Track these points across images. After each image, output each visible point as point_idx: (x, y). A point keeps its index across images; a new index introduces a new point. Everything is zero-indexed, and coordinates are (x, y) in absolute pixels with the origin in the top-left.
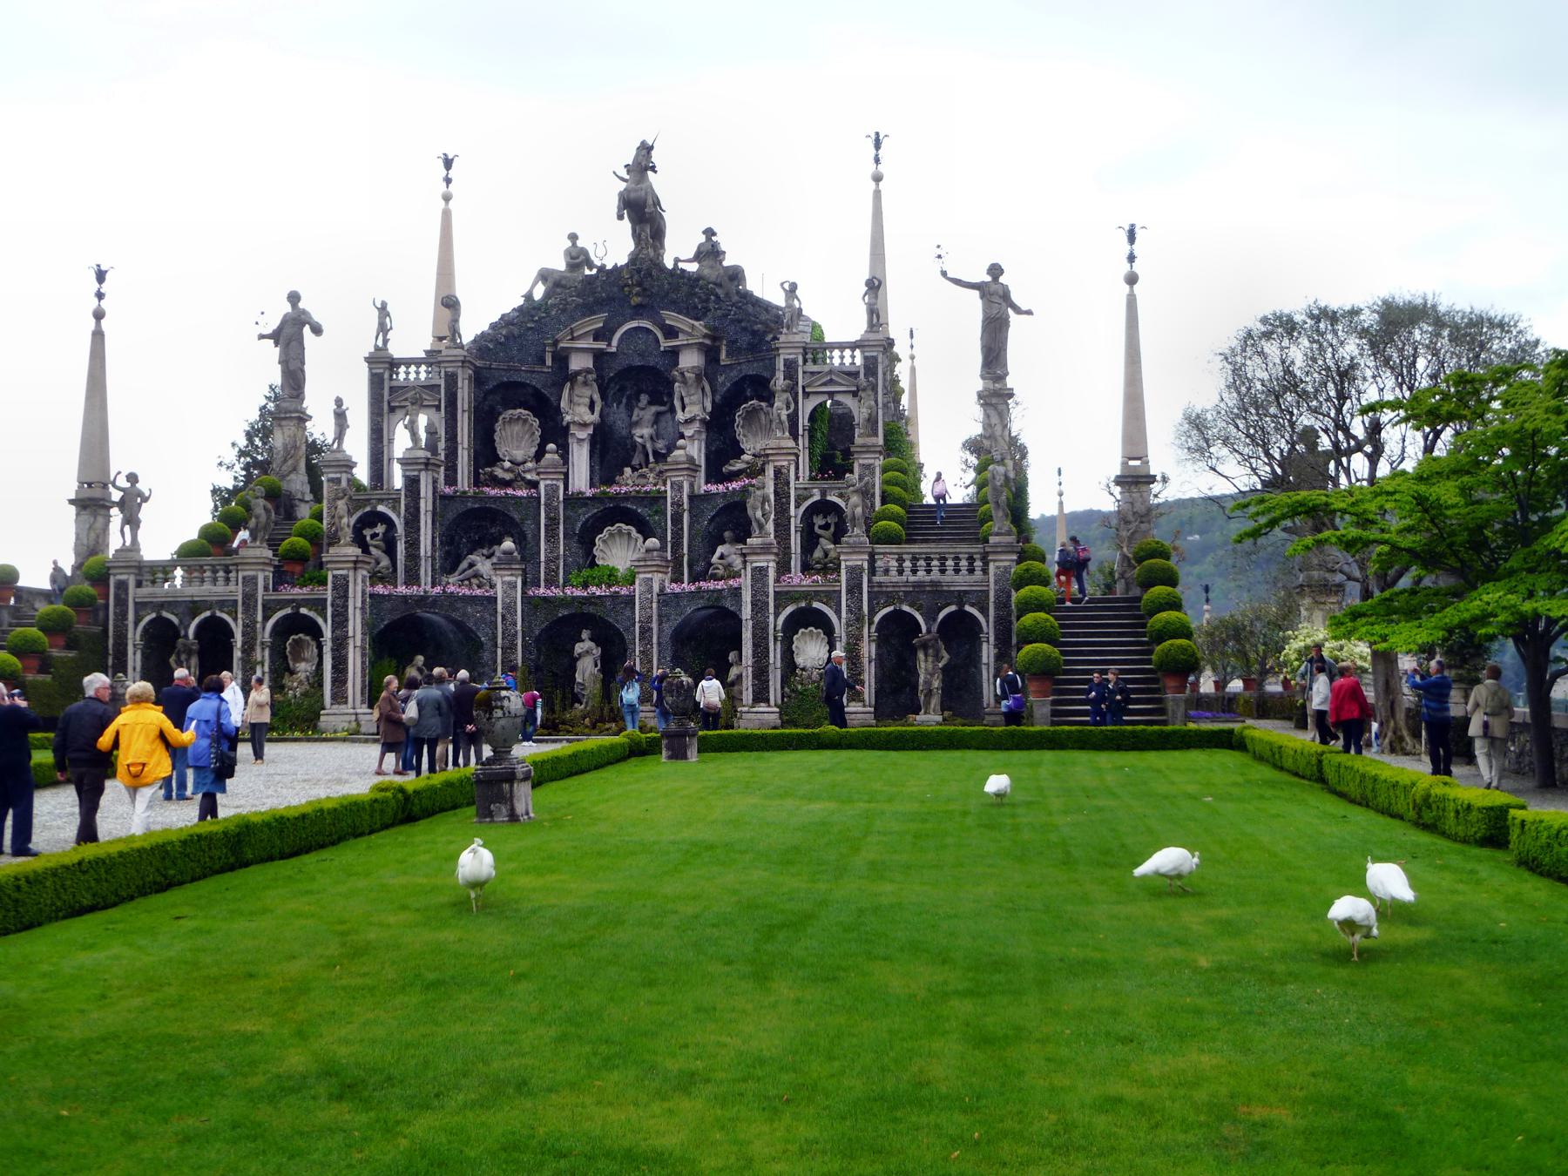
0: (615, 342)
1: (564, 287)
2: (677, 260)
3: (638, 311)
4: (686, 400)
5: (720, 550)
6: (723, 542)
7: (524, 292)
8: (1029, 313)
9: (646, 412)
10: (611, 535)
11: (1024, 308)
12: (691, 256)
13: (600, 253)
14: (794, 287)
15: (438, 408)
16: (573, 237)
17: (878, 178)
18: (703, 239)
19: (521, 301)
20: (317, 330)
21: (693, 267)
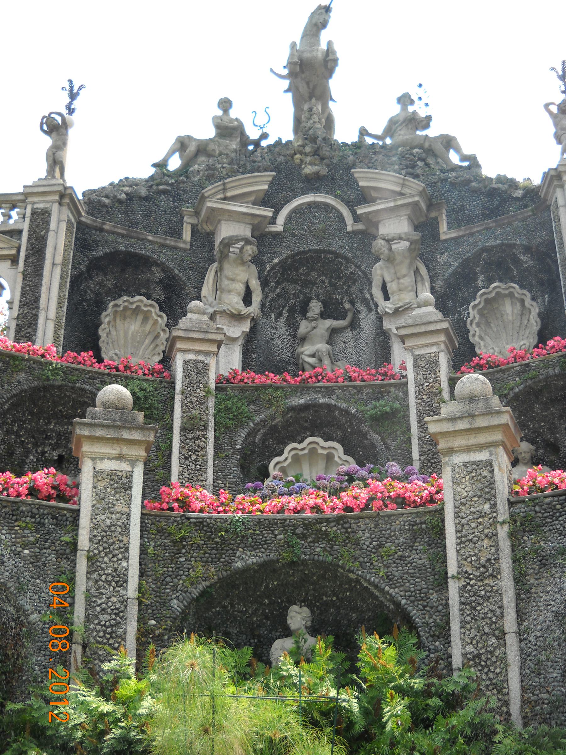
0: (281, 219)
1: (210, 155)
2: (363, 132)
3: (313, 183)
4: (392, 287)
7: (157, 160)
10: (297, 459)
12: (377, 128)
13: (261, 119)
15: (14, 260)
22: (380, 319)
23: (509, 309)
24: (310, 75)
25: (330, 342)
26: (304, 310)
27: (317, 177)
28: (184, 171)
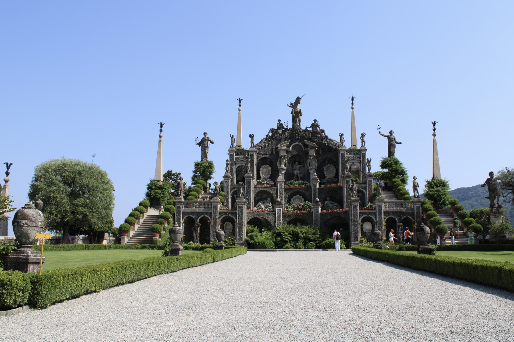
2: (306, 128)
3: (297, 140)
4: (311, 164)
5: (326, 202)
6: (326, 200)
8: (400, 143)
9: (297, 166)
11: (399, 142)
13: (286, 125)
14: (342, 135)
16: (279, 121)
17: (353, 108)
18: (313, 122)
19: (265, 137)
20: (212, 143)
21: (311, 129)
22: (308, 170)
23: (331, 168)
24: (296, 115)
25: (299, 169)
26: (295, 164)
27: (298, 139)
28: (273, 135)
